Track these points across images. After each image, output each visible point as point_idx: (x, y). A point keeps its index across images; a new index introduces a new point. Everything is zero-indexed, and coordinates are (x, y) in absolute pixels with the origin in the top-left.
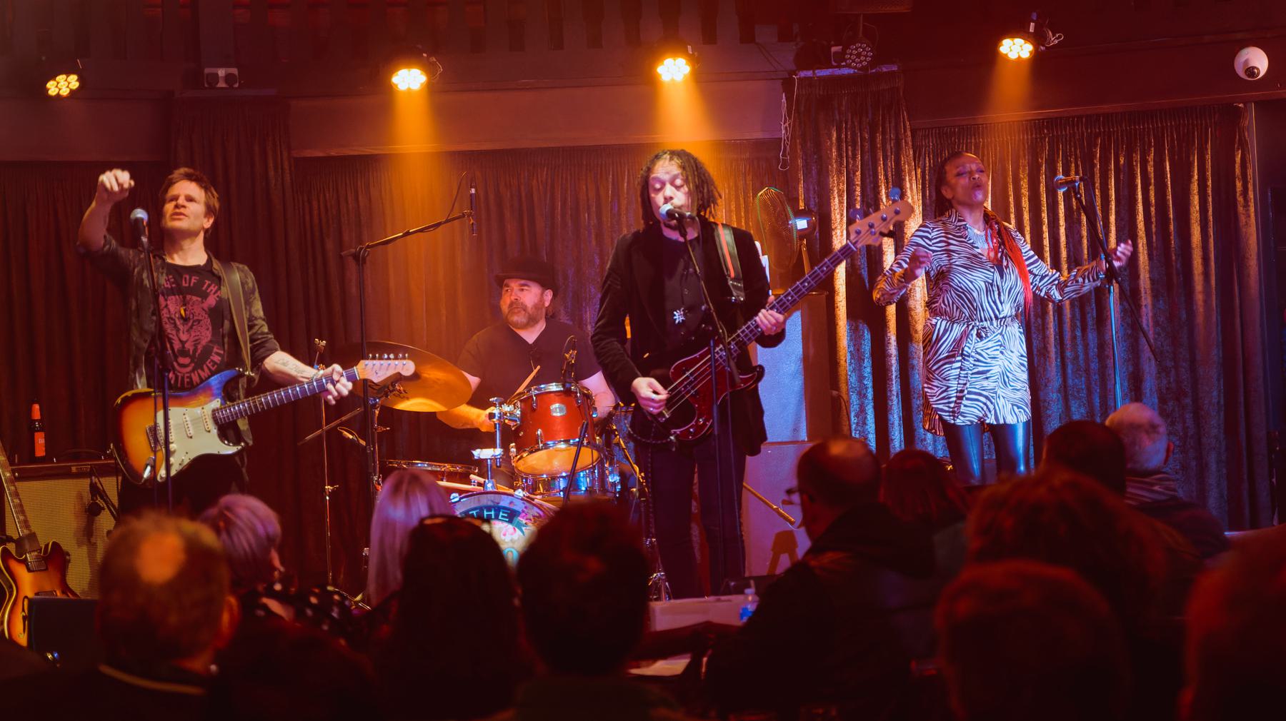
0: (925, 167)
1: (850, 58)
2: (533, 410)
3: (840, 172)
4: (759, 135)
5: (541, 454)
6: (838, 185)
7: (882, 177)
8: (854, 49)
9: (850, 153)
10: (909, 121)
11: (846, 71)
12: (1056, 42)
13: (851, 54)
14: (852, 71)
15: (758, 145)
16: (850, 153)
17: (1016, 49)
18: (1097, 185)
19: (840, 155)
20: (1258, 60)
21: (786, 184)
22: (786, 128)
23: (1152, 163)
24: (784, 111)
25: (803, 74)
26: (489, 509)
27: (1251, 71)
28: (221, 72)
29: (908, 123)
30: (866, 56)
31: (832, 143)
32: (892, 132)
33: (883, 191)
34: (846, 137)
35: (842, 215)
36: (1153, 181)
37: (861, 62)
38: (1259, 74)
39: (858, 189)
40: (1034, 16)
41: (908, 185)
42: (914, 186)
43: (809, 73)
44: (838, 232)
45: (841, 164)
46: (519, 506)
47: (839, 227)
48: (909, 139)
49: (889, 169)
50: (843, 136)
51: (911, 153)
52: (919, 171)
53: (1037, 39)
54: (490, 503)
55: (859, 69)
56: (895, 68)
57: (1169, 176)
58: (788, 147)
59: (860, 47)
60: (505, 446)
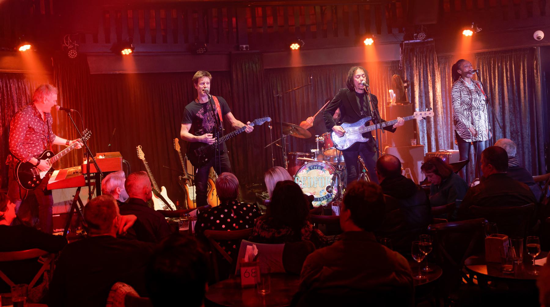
0: (441, 68)
1: (419, 37)
2: (328, 139)
3: (417, 69)
4: (394, 60)
5: (331, 151)
6: (416, 73)
7: (429, 71)
8: (420, 35)
9: (419, 64)
10: (437, 54)
11: (418, 41)
12: (480, 31)
13: (419, 36)
14: (420, 41)
15: (394, 63)
16: (419, 64)
17: (468, 33)
18: (492, 72)
19: (417, 65)
20: (541, 34)
21: (401, 73)
22: (401, 57)
23: (508, 65)
24: (401, 53)
25: (406, 42)
26: (315, 166)
27: (539, 38)
28: (244, 46)
29: (436, 55)
30: (424, 36)
31: (414, 61)
32: (432, 57)
33: (429, 75)
34: (418, 60)
35: (417, 81)
36: (509, 70)
37: (422, 38)
38: (541, 38)
39: (422, 74)
40: (473, 24)
41: (436, 73)
42: (438, 73)
43: (408, 42)
44: (416, 86)
45: (417, 67)
46: (324, 165)
47: (416, 85)
48: (437, 60)
49: (431, 68)
50: (417, 59)
51: (437, 63)
52: (440, 69)
53: (474, 30)
54: (316, 165)
55: (422, 40)
56: (432, 39)
57: (514, 69)
58: (402, 63)
59: (422, 34)
60: (320, 149)
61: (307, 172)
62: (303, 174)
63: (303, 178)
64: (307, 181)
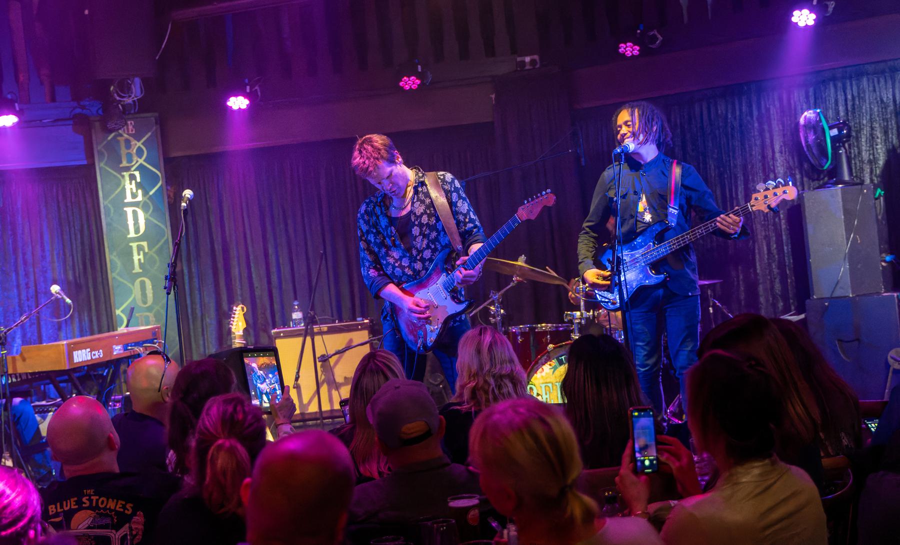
61: (552, 370)
62: (542, 377)
63: (543, 386)
64: (555, 394)
